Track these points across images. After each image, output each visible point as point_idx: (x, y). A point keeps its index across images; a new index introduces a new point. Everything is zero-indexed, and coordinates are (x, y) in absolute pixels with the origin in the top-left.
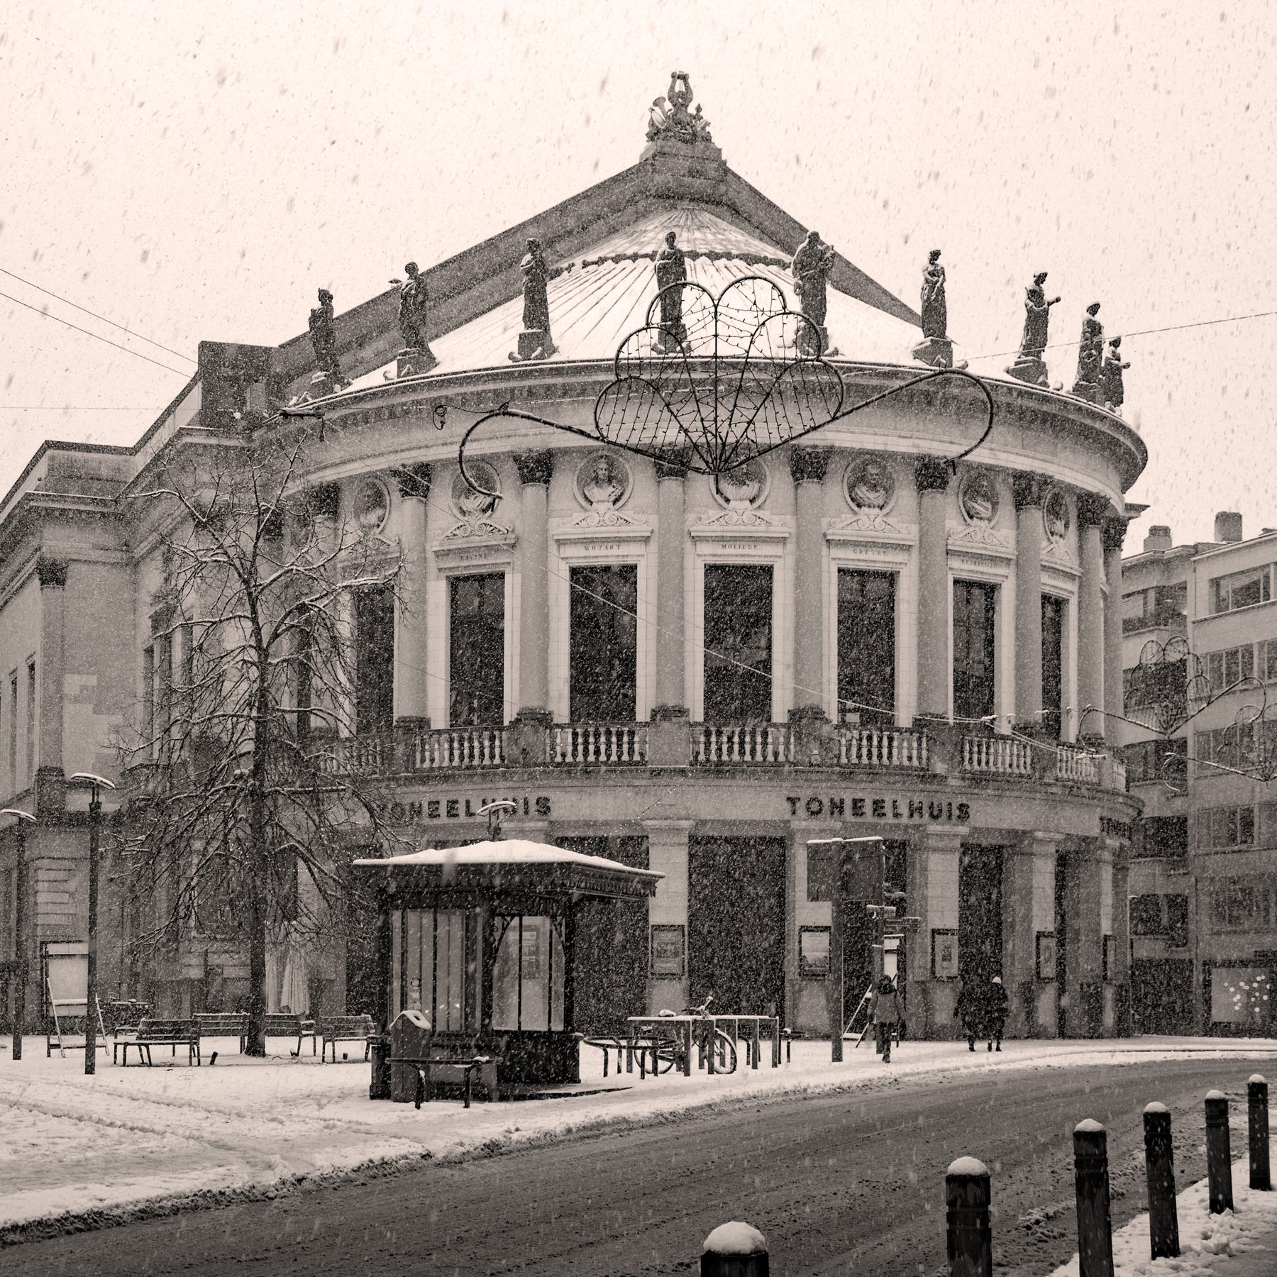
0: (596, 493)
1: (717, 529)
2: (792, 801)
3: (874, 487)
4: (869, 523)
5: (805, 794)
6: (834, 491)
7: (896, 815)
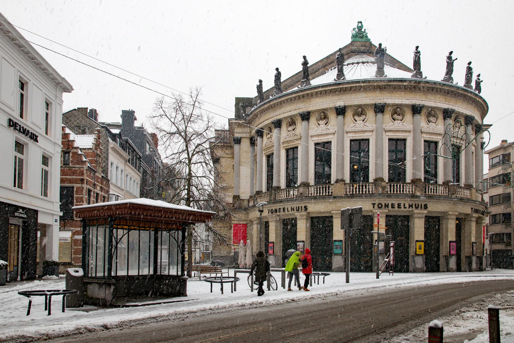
0: (321, 122)
1: (354, 129)
2: (374, 204)
3: (399, 115)
4: (398, 125)
5: (377, 202)
6: (387, 116)
7: (405, 208)
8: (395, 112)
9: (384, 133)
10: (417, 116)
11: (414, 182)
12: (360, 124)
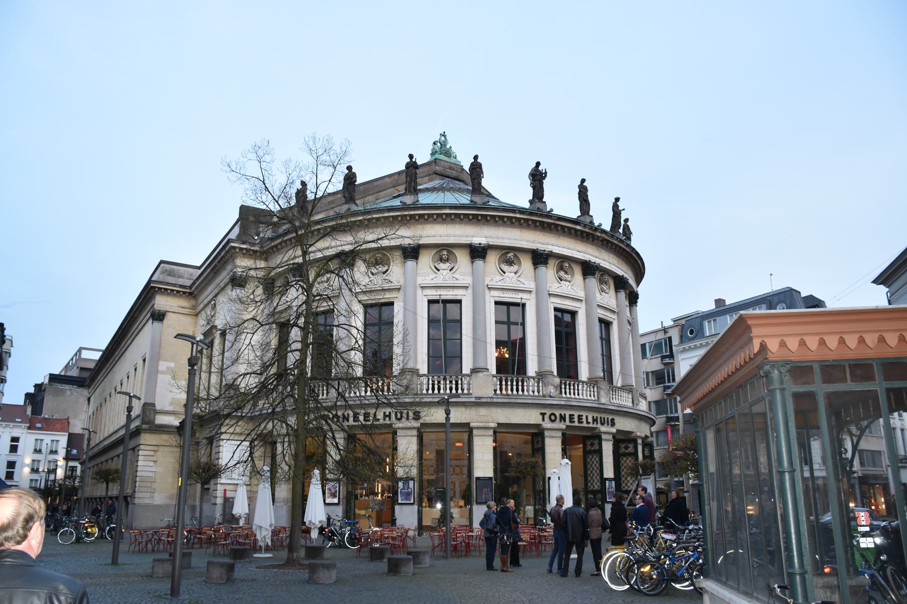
9: (487, 291)
10: (542, 269)
11: (541, 376)
12: (444, 275)
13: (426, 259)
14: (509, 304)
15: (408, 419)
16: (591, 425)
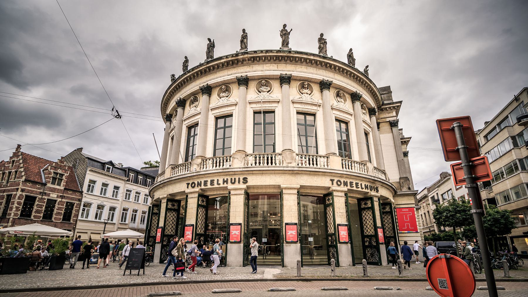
4: (306, 98)
8: (303, 86)
9: (291, 104)
10: (326, 92)
13: (253, 86)
14: (305, 114)
15: (239, 183)
16: (364, 190)
